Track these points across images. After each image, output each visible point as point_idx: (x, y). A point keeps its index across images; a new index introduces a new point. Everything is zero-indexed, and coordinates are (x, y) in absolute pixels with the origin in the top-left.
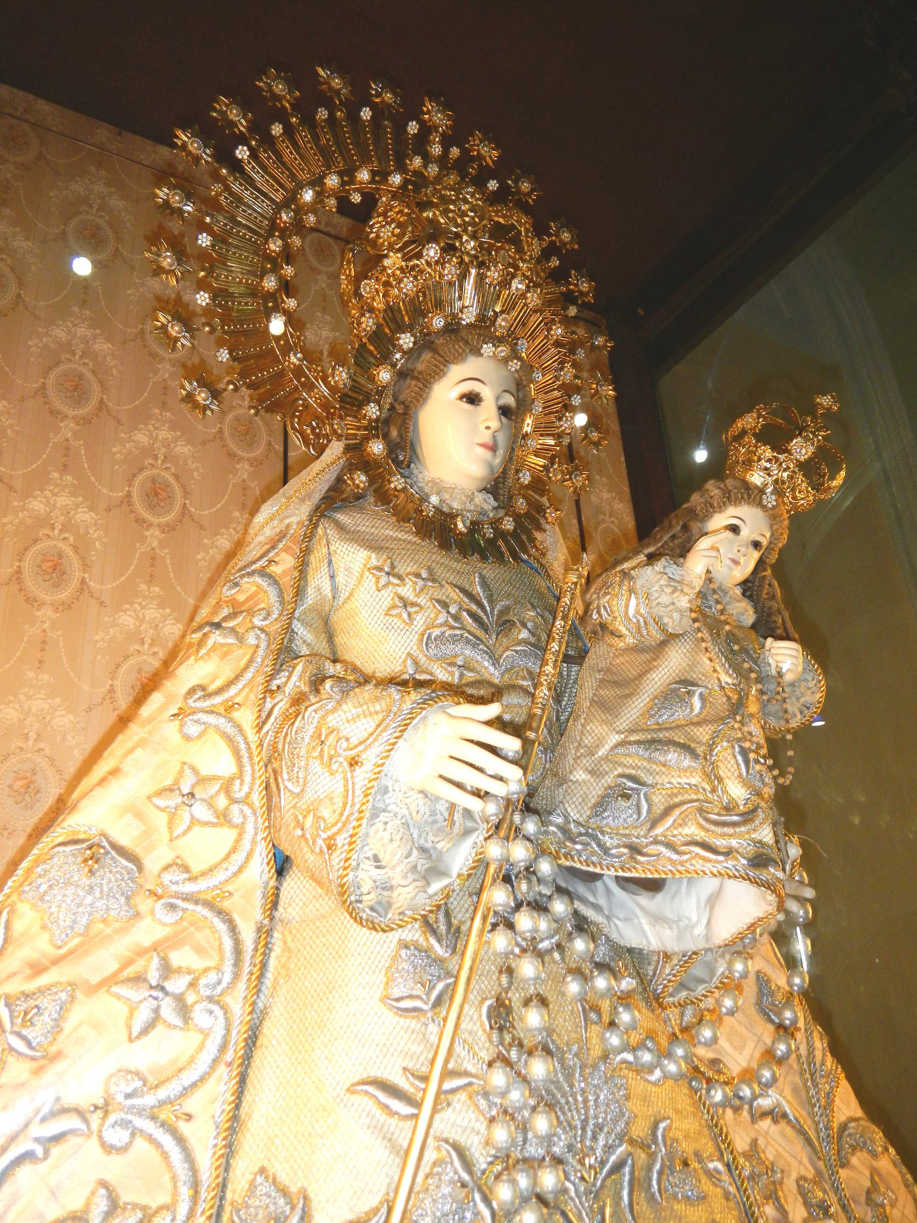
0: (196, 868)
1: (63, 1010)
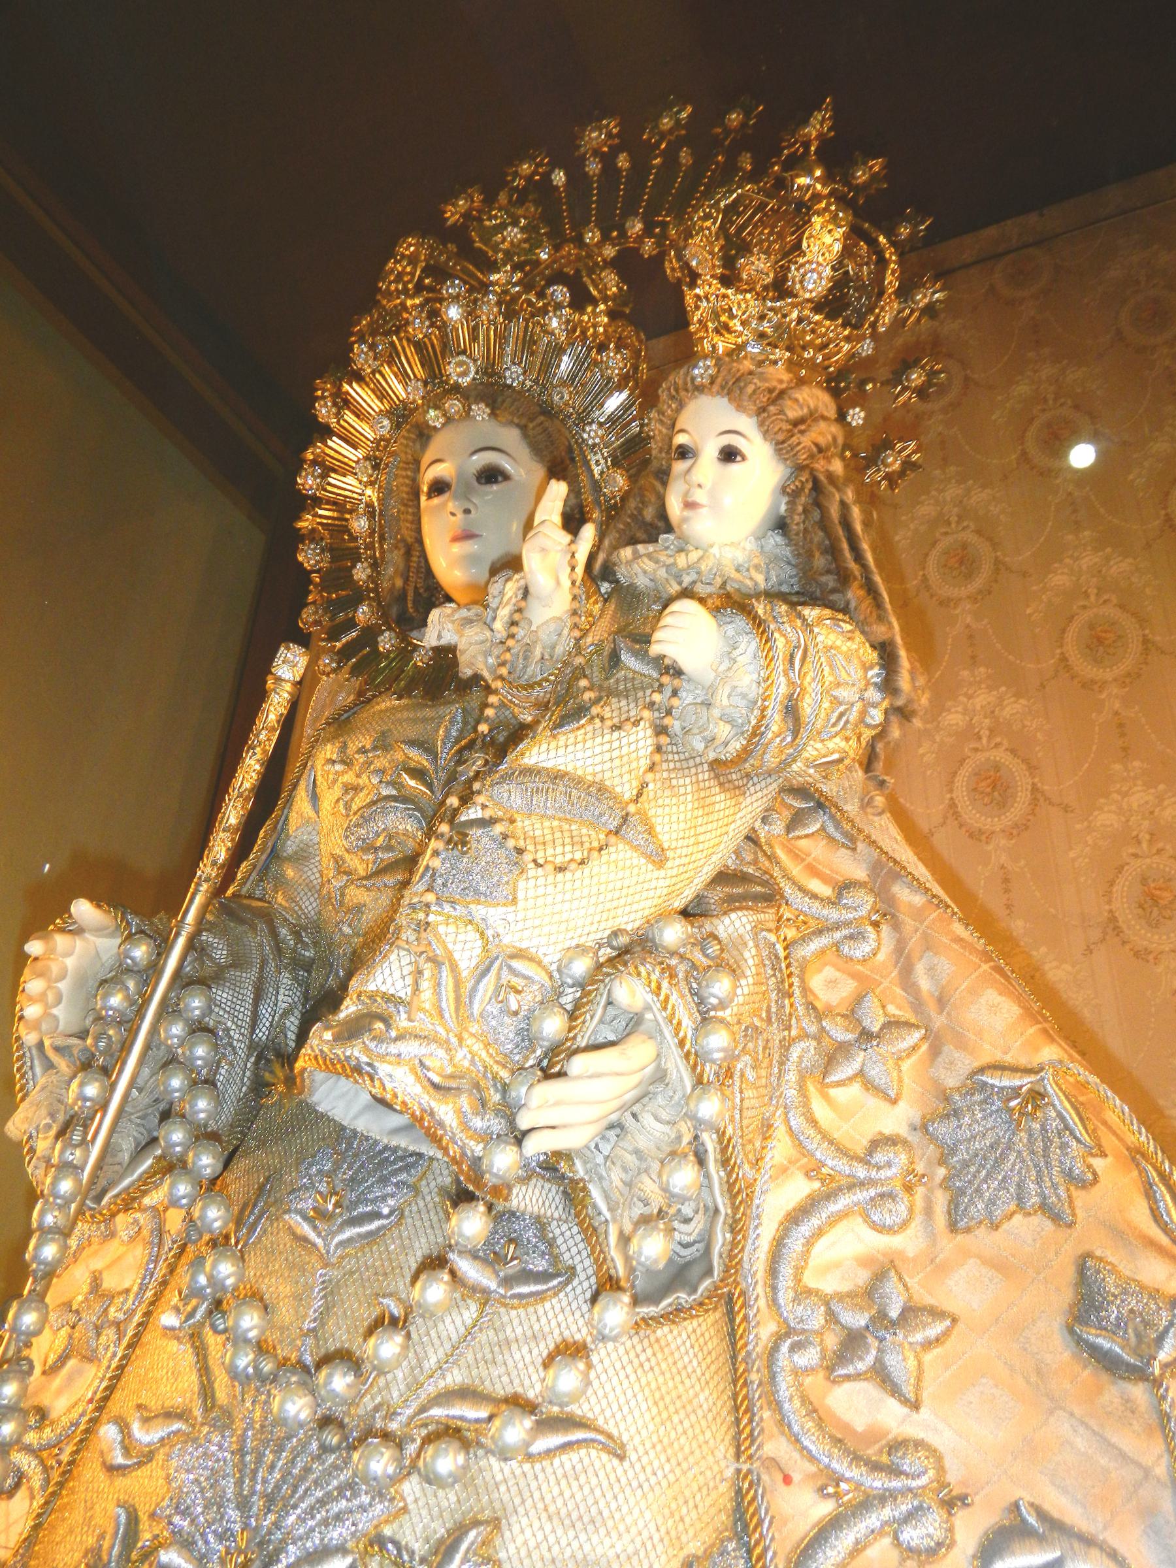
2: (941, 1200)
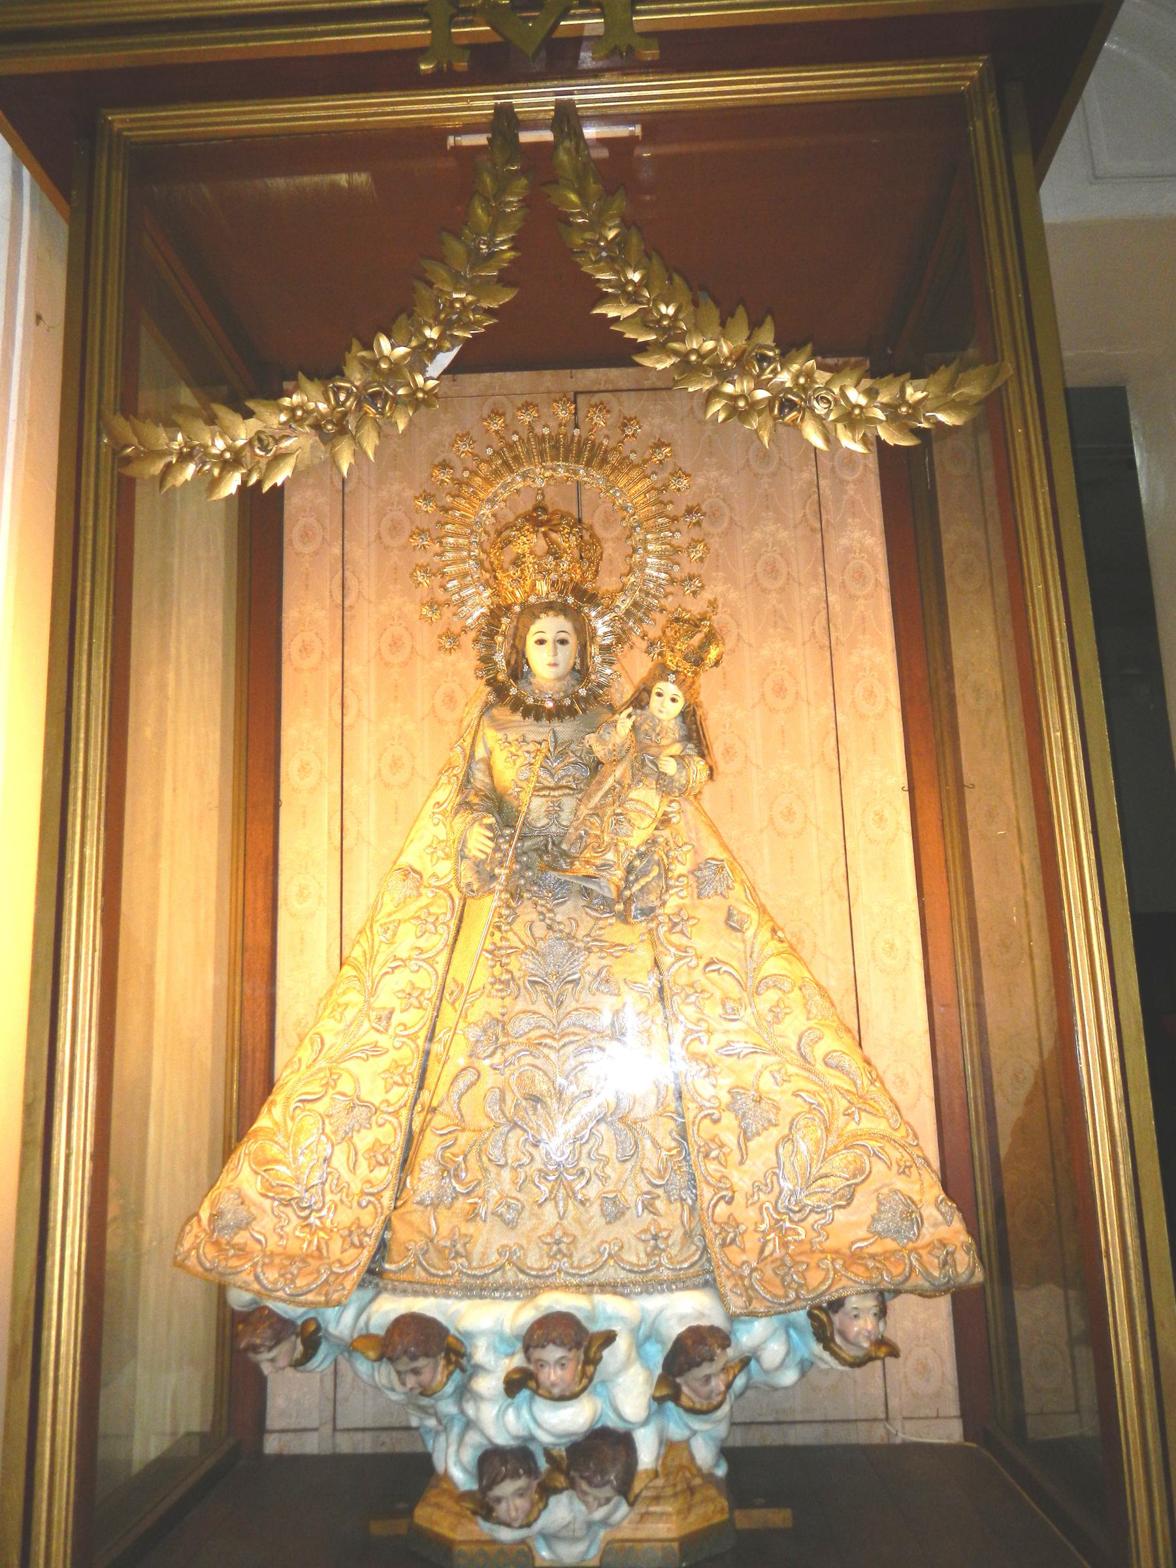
0: (441, 876)
1: (397, 927)
2: (696, 891)
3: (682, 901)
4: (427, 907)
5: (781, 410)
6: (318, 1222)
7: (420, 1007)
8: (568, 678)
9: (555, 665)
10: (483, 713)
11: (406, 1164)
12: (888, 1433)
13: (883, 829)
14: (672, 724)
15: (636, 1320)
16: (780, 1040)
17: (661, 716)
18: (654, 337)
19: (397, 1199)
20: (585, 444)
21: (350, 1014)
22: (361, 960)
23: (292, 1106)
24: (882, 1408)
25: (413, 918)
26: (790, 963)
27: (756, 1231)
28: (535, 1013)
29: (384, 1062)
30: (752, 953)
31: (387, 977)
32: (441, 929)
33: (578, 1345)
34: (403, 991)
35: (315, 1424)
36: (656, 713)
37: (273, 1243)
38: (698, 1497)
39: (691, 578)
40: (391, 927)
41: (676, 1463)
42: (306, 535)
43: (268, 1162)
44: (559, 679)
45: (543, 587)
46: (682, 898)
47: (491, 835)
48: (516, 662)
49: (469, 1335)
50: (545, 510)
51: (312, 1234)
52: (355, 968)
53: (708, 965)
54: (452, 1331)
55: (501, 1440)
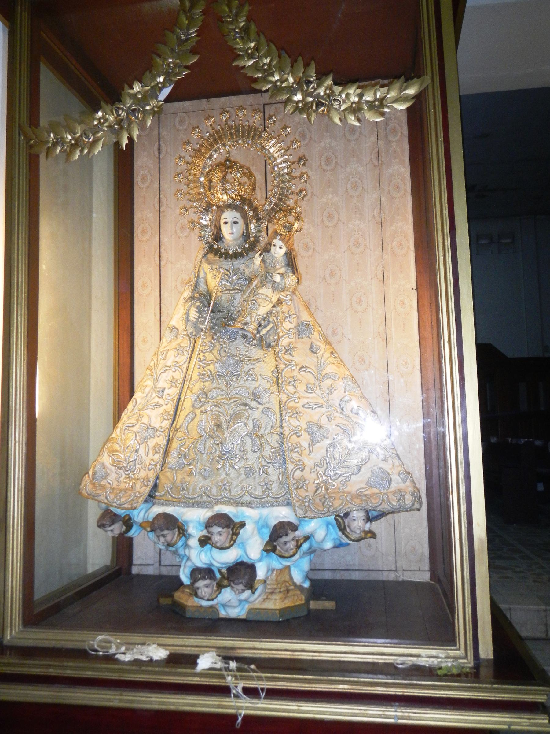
1: (167, 353)
2: (297, 335)
3: (291, 340)
4: (179, 344)
5: (316, 107)
6: (133, 476)
7: (176, 387)
8: (241, 239)
9: (232, 233)
10: (203, 257)
11: (166, 453)
12: (396, 576)
13: (404, 308)
14: (281, 259)
15: (258, 517)
16: (331, 401)
17: (276, 255)
18: (261, 75)
19: (162, 467)
20: (251, 129)
21: (147, 390)
22: (153, 367)
23: (124, 428)
24: (395, 566)
25: (174, 348)
26: (339, 367)
27: (314, 483)
28: (219, 389)
29: (161, 410)
30: (321, 362)
31: (163, 374)
32: (185, 353)
33: (228, 527)
34: (169, 380)
35: (151, 562)
36: (273, 253)
37: (115, 485)
38: (291, 593)
39: (301, 191)
40: (165, 353)
41: (283, 580)
42: (144, 179)
43: (113, 451)
44: (235, 240)
45: (225, 197)
46: (291, 339)
47: (197, 310)
48: (217, 233)
49: (187, 522)
50: (230, 161)
51: (130, 481)
52: (151, 371)
53: (300, 369)
54: (180, 521)
55: (199, 564)
